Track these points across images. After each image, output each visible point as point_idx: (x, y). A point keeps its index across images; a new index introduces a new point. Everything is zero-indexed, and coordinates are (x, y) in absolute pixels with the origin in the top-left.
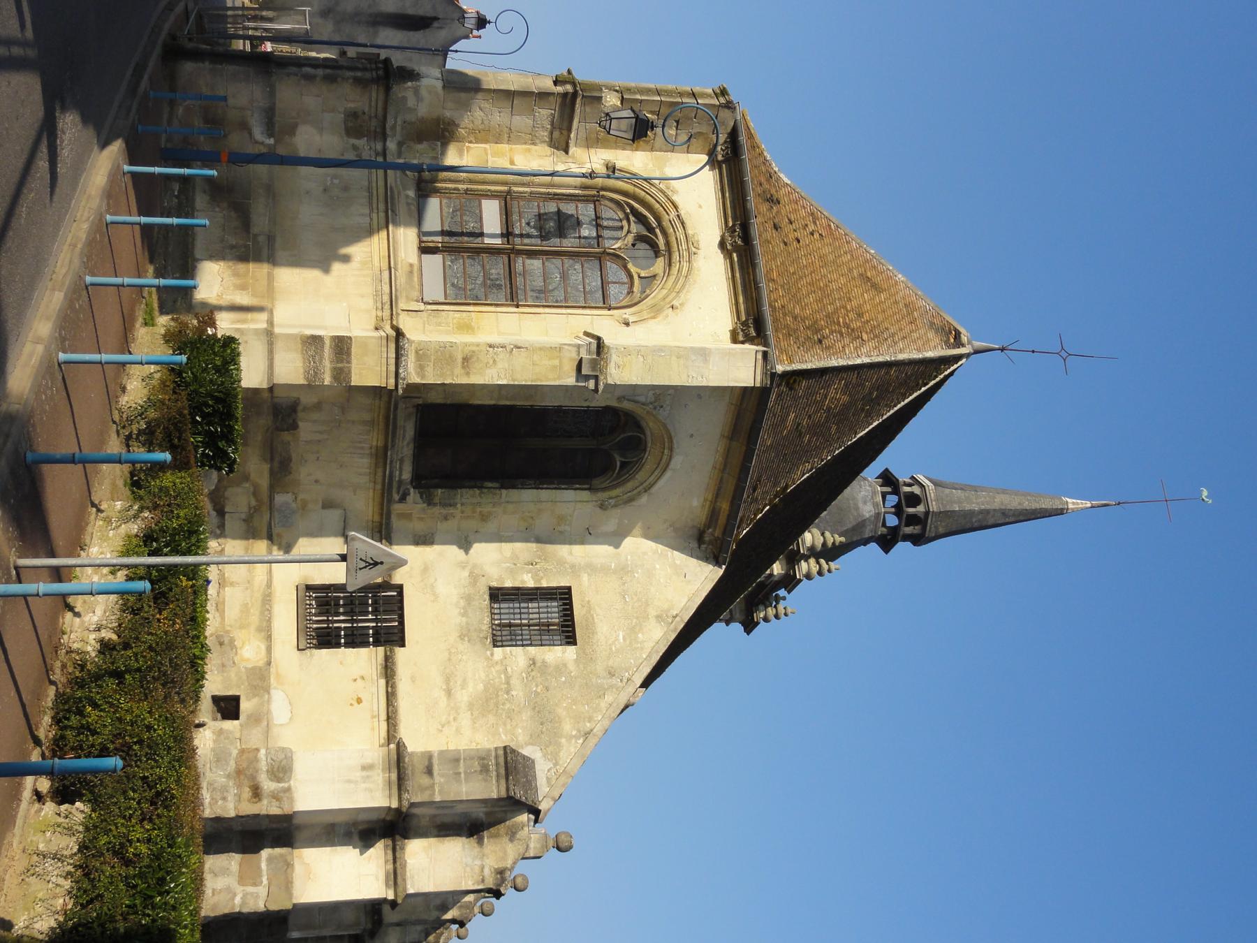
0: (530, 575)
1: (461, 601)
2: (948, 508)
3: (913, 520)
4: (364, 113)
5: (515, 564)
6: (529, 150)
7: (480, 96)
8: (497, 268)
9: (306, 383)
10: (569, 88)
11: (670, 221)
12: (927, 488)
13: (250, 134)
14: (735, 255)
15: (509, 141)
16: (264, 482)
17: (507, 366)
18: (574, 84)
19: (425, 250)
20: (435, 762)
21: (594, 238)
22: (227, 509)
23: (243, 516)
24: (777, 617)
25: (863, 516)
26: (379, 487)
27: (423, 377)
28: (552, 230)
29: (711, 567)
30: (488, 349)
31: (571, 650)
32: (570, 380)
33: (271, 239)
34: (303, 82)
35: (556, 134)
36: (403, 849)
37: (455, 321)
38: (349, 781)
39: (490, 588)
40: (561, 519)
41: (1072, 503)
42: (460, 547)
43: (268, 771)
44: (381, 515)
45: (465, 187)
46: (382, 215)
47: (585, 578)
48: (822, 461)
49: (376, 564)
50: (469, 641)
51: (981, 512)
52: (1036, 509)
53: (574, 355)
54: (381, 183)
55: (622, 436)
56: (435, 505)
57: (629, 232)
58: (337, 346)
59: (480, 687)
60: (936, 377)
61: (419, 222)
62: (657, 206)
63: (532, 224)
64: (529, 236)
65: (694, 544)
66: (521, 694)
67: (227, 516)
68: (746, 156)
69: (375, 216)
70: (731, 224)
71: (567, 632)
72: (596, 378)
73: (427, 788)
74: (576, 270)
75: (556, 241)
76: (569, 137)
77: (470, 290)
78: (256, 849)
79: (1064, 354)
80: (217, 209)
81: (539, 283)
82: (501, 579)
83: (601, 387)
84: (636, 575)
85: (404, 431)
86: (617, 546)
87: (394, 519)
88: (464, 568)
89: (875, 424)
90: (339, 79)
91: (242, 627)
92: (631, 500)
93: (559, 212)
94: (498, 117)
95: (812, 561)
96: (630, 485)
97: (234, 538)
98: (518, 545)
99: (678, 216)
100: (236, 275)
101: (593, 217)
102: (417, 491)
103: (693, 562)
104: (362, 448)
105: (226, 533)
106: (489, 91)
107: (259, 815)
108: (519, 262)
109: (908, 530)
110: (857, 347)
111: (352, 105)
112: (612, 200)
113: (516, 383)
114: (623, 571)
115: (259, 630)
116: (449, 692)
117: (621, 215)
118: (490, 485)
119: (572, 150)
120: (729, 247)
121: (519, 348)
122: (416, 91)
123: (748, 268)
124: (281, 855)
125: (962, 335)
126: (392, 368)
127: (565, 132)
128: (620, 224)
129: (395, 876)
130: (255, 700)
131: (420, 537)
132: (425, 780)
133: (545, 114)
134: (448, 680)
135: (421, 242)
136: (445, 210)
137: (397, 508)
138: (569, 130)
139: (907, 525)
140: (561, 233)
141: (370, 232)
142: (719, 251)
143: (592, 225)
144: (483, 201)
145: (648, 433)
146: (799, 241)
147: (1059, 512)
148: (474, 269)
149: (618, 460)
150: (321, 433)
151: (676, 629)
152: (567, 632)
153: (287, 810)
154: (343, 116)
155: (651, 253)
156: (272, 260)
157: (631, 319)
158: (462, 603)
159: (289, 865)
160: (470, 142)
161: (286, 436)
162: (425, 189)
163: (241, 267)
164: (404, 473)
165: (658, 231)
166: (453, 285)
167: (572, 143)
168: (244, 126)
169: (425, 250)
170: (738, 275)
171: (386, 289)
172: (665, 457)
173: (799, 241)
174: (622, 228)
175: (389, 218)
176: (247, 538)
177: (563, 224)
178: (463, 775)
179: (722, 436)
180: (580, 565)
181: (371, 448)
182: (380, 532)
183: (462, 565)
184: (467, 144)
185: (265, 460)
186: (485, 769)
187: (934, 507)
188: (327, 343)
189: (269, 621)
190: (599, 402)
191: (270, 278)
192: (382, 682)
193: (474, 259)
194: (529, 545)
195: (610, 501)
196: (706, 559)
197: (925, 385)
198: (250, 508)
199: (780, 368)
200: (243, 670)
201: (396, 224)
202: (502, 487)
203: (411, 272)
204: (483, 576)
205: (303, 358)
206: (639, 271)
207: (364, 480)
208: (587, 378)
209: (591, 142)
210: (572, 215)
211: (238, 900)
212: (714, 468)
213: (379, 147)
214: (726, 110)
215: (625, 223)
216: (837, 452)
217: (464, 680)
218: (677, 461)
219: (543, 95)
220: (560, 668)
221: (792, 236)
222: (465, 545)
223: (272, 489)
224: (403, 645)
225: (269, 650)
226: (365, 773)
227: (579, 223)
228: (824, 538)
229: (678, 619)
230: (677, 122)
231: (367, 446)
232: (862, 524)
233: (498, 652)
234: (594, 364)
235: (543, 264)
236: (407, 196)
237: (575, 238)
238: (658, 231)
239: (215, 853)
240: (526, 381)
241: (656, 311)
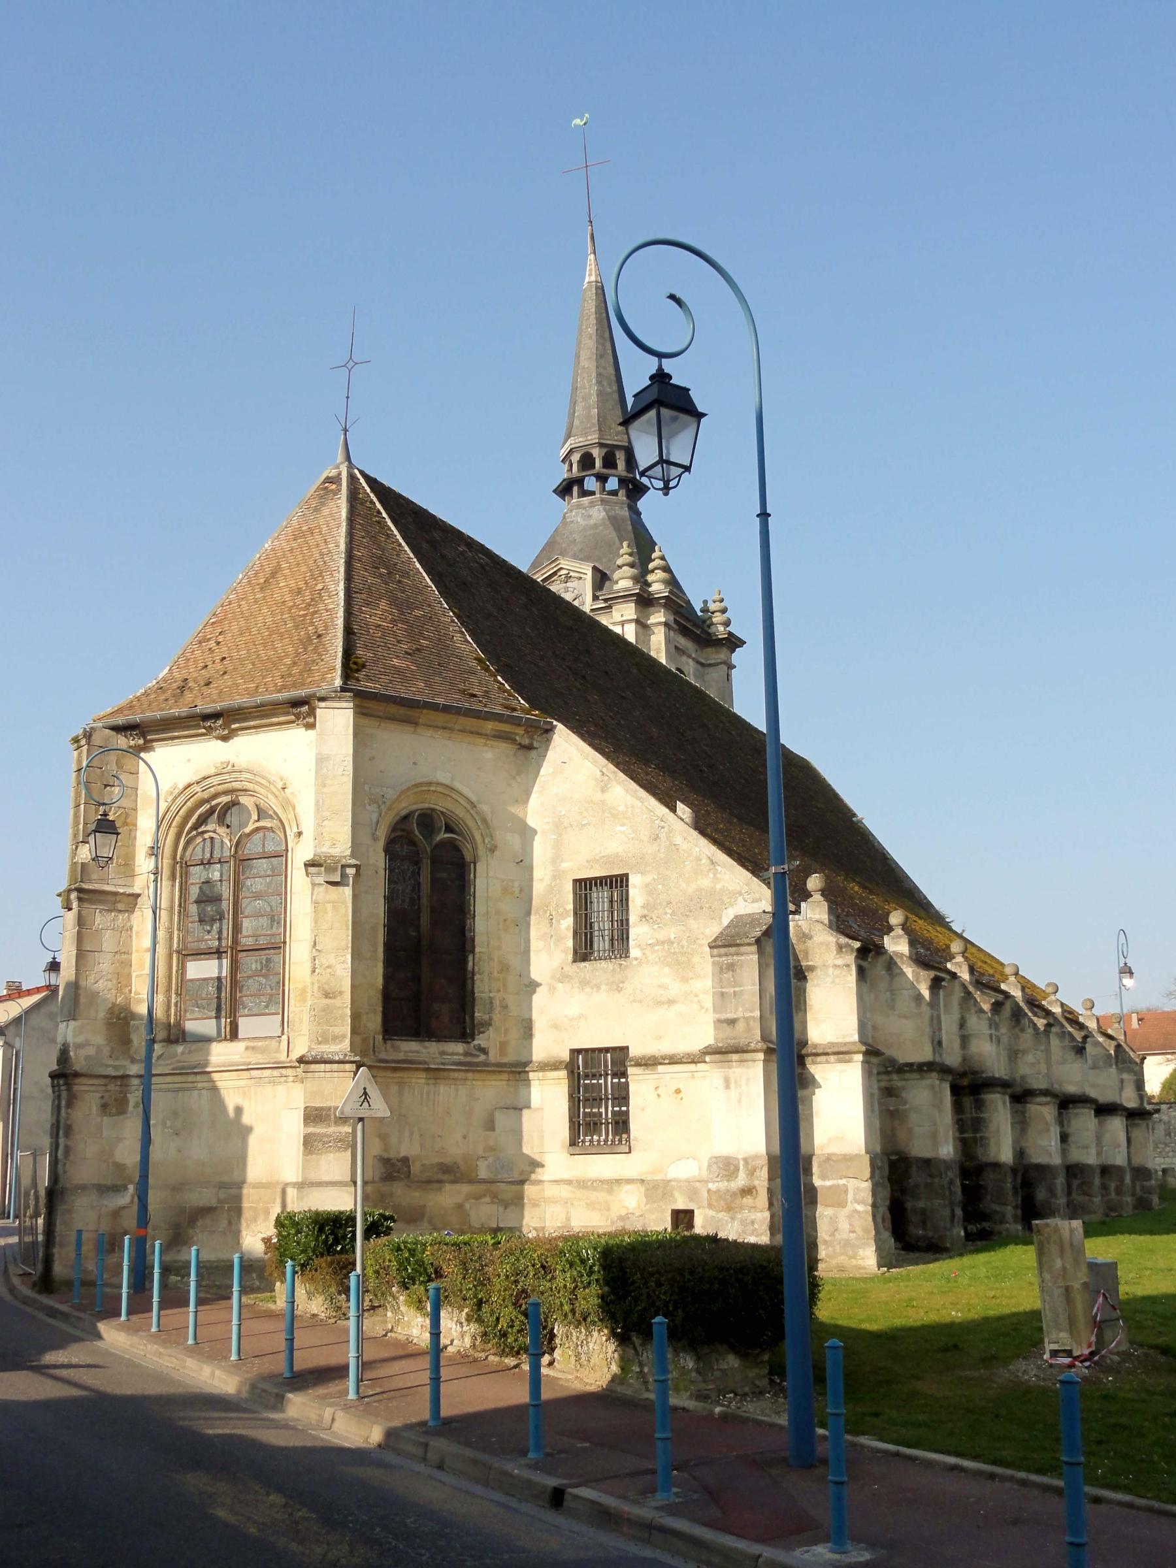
0: (562, 922)
1: (586, 990)
2: (595, 421)
3: (609, 462)
4: (102, 1097)
5: (552, 936)
6: (137, 933)
7: (82, 983)
8: (250, 963)
9: (350, 1150)
10: (74, 895)
11: (203, 791)
12: (573, 446)
13: (124, 1208)
14: (233, 726)
15: (129, 953)
16: (465, 1189)
17: (333, 955)
18: (69, 891)
19: (234, 1035)
20: (724, 1016)
21: (221, 866)
22: (495, 1226)
23: (501, 1209)
24: (724, 611)
25: (603, 519)
26: (470, 1075)
27: (344, 1036)
28: (214, 908)
29: (555, 737)
30: (316, 974)
31: (633, 880)
32: (347, 891)
33: (222, 1186)
34: (72, 1157)
35: (120, 906)
36: (816, 1046)
37: (297, 1005)
38: (740, 1101)
39: (575, 961)
40: (506, 891)
41: (590, 277)
42: (534, 992)
43: (728, 1181)
44: (500, 1072)
45: (174, 996)
46: (199, 1078)
47: (565, 865)
48: (453, 621)
49: (365, 1093)
50: (623, 982)
51: (599, 382)
52: (597, 319)
53: (322, 889)
54: (169, 1079)
55: (417, 833)
56: (491, 1019)
57: (214, 832)
58: (314, 1121)
59: (666, 970)
60: (372, 502)
61: (208, 1040)
62: (189, 804)
63: (208, 928)
64: (220, 932)
65: (534, 753)
66: (673, 929)
67: (501, 1225)
68: (137, 718)
69: (200, 1085)
70: (203, 731)
71: (618, 882)
72: (343, 867)
73: (748, 1025)
74: (254, 884)
75: (224, 904)
76: (122, 894)
77: (272, 990)
78: (812, 1191)
79: (350, 364)
80: (195, 1239)
81: (264, 921)
82: (565, 951)
83: (353, 862)
84: (563, 813)
85: (411, 1051)
86: (535, 832)
87: (505, 1060)
88: (554, 988)
89: (418, 565)
90: (69, 1122)
91: (608, 1209)
92: (485, 821)
93: (197, 902)
94: (104, 964)
95: (650, 578)
96: (470, 823)
97: (522, 1218)
98: (533, 933)
99: (197, 783)
100: (255, 1219)
101: (202, 867)
102: (477, 1037)
103: (551, 755)
104: (428, 1093)
105: (518, 1226)
106: (77, 975)
107: (768, 1189)
108: (246, 941)
109: (621, 465)
110: (329, 596)
111: (94, 1110)
112: (185, 849)
113: (350, 945)
114: (559, 827)
115: (610, 1191)
116: (671, 1002)
117: (199, 840)
118: (470, 964)
119: (136, 890)
120: (226, 732)
121: (315, 944)
122: (79, 1046)
123: (245, 713)
124: (820, 1166)
125: (330, 475)
126: (335, 1066)
127: (118, 898)
128: (208, 843)
129: (841, 1053)
130: (676, 1194)
131: (525, 1033)
132: (740, 1026)
133: (100, 919)
134: (660, 1003)
135: (226, 1039)
136: (197, 1015)
137: (493, 1057)
138: (116, 894)
139: (615, 466)
140: (217, 899)
141: (215, 1089)
142: (231, 741)
143: (209, 868)
144: (188, 978)
145: (414, 807)
146: (224, 658)
147: (600, 291)
148: (251, 986)
149: (443, 835)
150: (412, 1133)
151: (614, 772)
152: (618, 882)
153: (763, 1161)
154: (105, 1118)
155: (234, 810)
156: (240, 1184)
157: (295, 830)
158: (587, 989)
159: (829, 1158)
160: (130, 991)
161: (415, 1168)
162: (177, 1035)
163: (247, 1214)
164: (456, 1051)
165: (213, 803)
166: (267, 1007)
167: (129, 891)
168: (116, 1214)
169: (234, 1035)
170: (252, 723)
171: (267, 1073)
172: (439, 789)
173: (224, 658)
174: (212, 838)
175: (199, 1071)
176: (522, 1206)
177: (208, 897)
178: (736, 989)
179: (414, 733)
180: (552, 871)
181: (428, 1084)
182: (520, 1073)
183: (552, 989)
184: (132, 995)
185: (440, 1189)
186: (731, 967)
187: (594, 438)
188: (310, 1130)
189: (602, 1182)
190: (378, 860)
191: (258, 1186)
192: (660, 1068)
193: (242, 986)
194: (532, 923)
195: (486, 841)
196: (549, 741)
197: (379, 512)
198: (493, 1203)
199: (338, 682)
200: (648, 1207)
201: (207, 1064)
202: (473, 951)
203: (253, 1048)
204: (562, 968)
205: (327, 1152)
206: (252, 821)
207: (463, 1090)
208: (344, 876)
209: (128, 868)
210: (200, 888)
211: (860, 1208)
212: (449, 739)
214: (94, 737)
215: (206, 836)
216: (446, 606)
217: (660, 986)
218: (442, 777)
219: (81, 921)
220: (649, 889)
221: (219, 666)
222: (533, 986)
223: (471, 1181)
224: (627, 1048)
225: (629, 1181)
226: (733, 1085)
227: (207, 882)
228: (623, 565)
229: (604, 770)
230: (106, 786)
231: (426, 1088)
232: (614, 520)
233: (634, 952)
234: (330, 869)
235: (246, 917)
236: (183, 1053)
237: (221, 885)
238: (213, 803)
239: (816, 1230)
240: (348, 936)
241: (288, 805)
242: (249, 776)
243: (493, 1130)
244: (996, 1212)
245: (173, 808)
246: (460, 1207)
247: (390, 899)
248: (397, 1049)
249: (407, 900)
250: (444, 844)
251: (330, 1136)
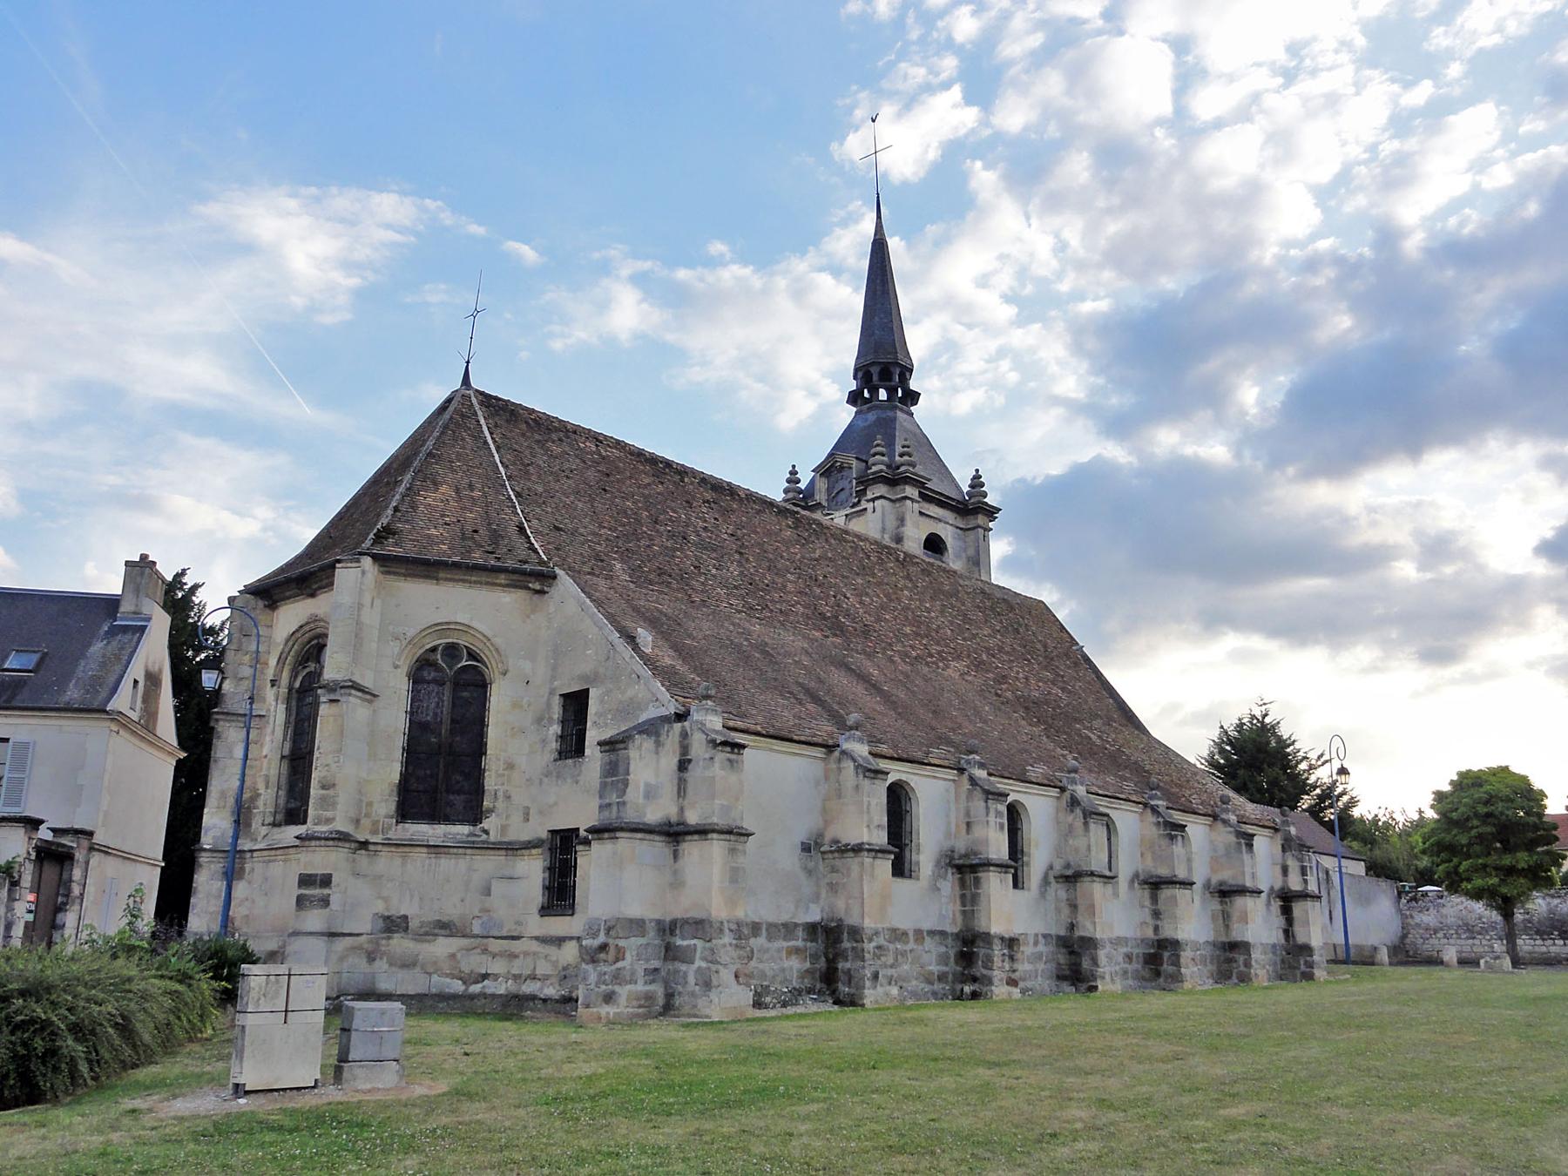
54: (266, 853)
58: (305, 885)
126: (323, 843)
150: (412, 896)
161: (413, 924)
179: (437, 584)
202: (485, 754)
213: (248, 855)
225: (571, 938)
242: (322, 624)
243: (490, 895)
244: (984, 976)
245: (287, 650)
246: (453, 956)
247: (412, 714)
248: (404, 830)
251: (315, 896)
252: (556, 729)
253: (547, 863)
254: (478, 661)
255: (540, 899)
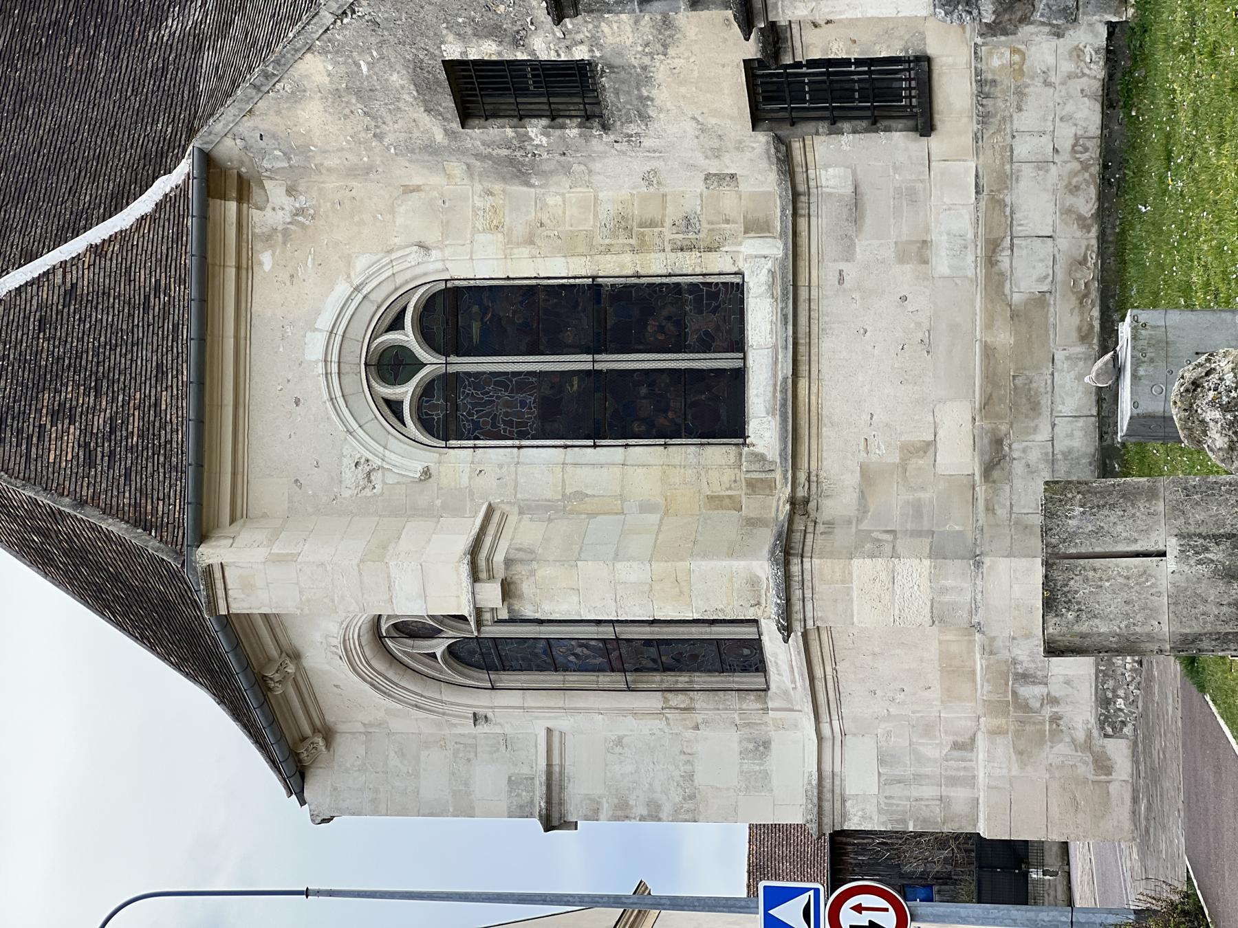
31: (453, 51)
158: (651, 112)
249: (519, 396)
250: (426, 335)
252: (535, 130)
253: (823, 126)
254: (404, 310)
255: (896, 135)
